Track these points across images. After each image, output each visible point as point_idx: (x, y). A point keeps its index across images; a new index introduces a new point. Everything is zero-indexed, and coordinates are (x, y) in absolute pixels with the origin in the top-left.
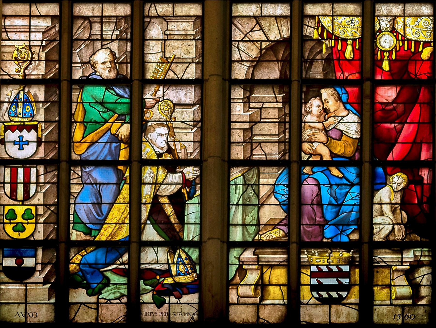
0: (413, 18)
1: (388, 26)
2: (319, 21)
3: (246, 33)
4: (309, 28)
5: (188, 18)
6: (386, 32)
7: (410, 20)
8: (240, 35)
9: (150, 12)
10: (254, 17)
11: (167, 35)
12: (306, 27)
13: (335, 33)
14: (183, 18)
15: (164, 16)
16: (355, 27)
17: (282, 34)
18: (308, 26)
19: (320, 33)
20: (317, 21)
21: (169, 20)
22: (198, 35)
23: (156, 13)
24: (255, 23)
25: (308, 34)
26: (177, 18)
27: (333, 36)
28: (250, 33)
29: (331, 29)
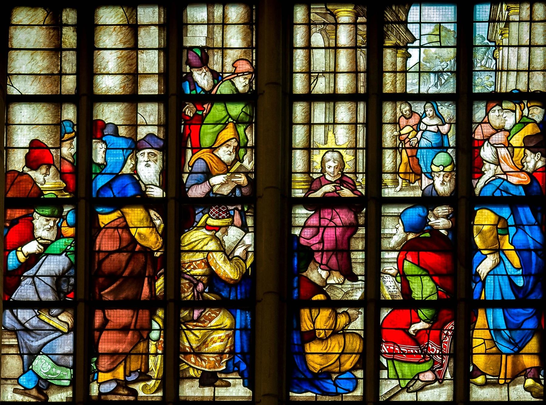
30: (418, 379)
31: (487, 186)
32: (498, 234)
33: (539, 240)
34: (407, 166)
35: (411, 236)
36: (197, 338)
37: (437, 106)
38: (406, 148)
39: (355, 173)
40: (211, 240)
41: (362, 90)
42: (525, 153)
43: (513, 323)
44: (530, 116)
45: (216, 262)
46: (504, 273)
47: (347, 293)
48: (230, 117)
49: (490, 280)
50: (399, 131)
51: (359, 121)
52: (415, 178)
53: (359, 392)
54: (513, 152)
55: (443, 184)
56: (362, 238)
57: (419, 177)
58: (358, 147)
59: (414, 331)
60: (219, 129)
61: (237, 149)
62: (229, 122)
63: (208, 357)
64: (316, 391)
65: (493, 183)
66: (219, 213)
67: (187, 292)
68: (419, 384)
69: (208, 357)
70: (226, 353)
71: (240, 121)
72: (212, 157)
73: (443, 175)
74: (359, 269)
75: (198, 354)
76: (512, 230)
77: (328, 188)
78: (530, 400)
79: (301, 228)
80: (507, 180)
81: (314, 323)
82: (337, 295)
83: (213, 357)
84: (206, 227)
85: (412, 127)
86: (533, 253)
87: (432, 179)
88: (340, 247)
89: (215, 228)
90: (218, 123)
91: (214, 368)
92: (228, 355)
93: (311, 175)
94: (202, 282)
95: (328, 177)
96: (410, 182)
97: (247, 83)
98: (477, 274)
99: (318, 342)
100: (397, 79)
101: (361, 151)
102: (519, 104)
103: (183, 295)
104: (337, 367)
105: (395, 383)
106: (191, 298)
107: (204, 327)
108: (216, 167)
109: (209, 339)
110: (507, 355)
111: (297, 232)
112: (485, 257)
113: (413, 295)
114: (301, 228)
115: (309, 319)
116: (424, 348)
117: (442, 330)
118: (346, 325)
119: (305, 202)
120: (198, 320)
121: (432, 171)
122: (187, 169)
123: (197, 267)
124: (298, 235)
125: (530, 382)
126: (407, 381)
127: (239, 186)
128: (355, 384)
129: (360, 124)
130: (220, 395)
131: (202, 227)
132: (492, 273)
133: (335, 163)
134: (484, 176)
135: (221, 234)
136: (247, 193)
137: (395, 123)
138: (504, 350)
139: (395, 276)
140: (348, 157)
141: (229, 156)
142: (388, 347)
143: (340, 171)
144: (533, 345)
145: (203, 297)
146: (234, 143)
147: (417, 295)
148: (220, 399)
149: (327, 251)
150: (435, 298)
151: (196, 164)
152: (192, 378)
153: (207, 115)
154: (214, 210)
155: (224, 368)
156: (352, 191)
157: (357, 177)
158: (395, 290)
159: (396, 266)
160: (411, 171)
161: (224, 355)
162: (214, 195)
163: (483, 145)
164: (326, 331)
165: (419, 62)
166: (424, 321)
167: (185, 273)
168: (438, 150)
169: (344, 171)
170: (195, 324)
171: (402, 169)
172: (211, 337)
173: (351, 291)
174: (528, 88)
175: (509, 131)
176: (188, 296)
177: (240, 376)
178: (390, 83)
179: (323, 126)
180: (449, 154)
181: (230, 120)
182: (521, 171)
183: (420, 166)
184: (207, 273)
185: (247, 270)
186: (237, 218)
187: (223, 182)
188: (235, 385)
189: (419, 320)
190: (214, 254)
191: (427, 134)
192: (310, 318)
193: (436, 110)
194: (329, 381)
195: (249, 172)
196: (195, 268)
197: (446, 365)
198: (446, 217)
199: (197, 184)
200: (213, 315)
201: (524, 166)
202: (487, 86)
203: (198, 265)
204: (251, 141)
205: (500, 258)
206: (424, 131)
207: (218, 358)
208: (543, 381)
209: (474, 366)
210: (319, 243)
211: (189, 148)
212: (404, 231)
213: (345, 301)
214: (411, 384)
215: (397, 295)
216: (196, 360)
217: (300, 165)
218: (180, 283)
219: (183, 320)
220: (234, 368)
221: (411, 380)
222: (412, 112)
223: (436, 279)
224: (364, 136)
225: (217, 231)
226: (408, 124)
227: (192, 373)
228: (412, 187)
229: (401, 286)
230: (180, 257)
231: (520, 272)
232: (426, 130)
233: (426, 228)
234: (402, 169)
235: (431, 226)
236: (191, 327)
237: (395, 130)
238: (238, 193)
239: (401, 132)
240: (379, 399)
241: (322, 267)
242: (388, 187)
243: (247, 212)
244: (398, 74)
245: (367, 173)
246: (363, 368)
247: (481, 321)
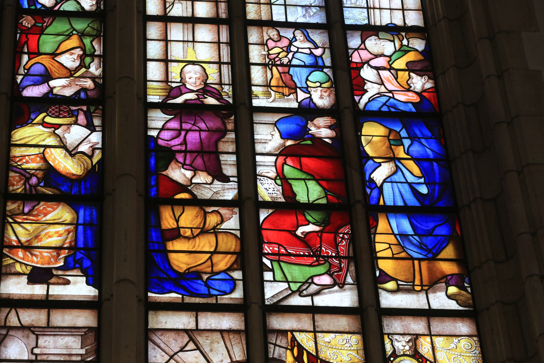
0: (445, 338)
1: (407, 348)
2: (294, 339)
3: (172, 353)
4: (277, 348)
5: (73, 330)
6: (405, 358)
7: (441, 340)
8: (162, 356)
9: (7, 320)
10: (186, 331)
11: (36, 355)
12: (272, 346)
13: (322, 356)
14: (65, 330)
15: (32, 327)
16: (353, 348)
17: (233, 356)
18: (275, 345)
19: (296, 355)
20: (289, 338)
21: (40, 333)
22: (89, 355)
23: (18, 322)
24: (186, 339)
25: (276, 356)
26: (55, 330)
27: (319, 361)
28: (180, 354)
29: (315, 350)
30: (313, 282)
31: (372, 102)
32: (391, 145)
33: (438, 151)
34: (279, 81)
35: (289, 143)
36: (27, 232)
37: (308, 33)
38: (277, 66)
39: (221, 84)
40: (50, 136)
41: (223, 15)
42: (409, 75)
43: (422, 230)
44: (410, 45)
45: (55, 158)
46: (403, 180)
47: (216, 193)
48: (74, 30)
49: (387, 187)
50: (268, 51)
51: (221, 41)
52: (289, 92)
53: (238, 294)
54: (397, 74)
55: (321, 97)
56: (232, 142)
57: (293, 91)
58: (222, 61)
59: (302, 233)
60: (61, 40)
61: (82, 58)
62: (73, 34)
63: (41, 253)
64: (183, 293)
65: (378, 99)
66: (59, 112)
67: (16, 185)
68: (313, 288)
69: (41, 253)
70: (65, 248)
71: (86, 34)
72: (53, 62)
73: (321, 91)
74: (230, 171)
75: (28, 248)
76: (407, 142)
77: (191, 96)
78: (456, 308)
79: (159, 130)
80: (393, 98)
81: (177, 221)
82: (205, 194)
83: (47, 252)
84: (44, 124)
85: (281, 48)
86: (435, 164)
87: (309, 93)
88: (206, 149)
89: (55, 126)
90: (61, 34)
91: (49, 264)
92: (67, 251)
93: (169, 84)
94: (36, 176)
95: (188, 86)
97: (94, 3)
98: (372, 181)
99: (183, 240)
100: (261, 9)
101: (226, 66)
102: (397, 35)
103: (11, 188)
104: (209, 267)
105: (285, 285)
106: (22, 191)
107: (37, 220)
108: (57, 71)
109: (43, 233)
110: (420, 260)
111: (154, 133)
112: (377, 165)
113: (298, 198)
114: (159, 130)
115: (171, 217)
116: (317, 251)
117: (336, 234)
118: (218, 225)
119: (163, 106)
120: (29, 214)
121: (308, 87)
122: (22, 71)
123: (31, 162)
124: (155, 137)
125: (453, 290)
126: (299, 285)
127: (84, 89)
128: (232, 286)
129: (223, 43)
130: (55, 293)
131: (38, 124)
132: (389, 180)
133: (196, 74)
134: (367, 93)
135: (61, 132)
136: (94, 96)
137: (263, 44)
138: (415, 255)
139: (275, 179)
140: (212, 70)
141: (73, 63)
142: (271, 248)
143: (203, 81)
144: (449, 252)
145: (36, 190)
146: (79, 52)
147: (302, 197)
148: (56, 298)
149: (191, 152)
150: (324, 201)
151: (33, 68)
152: (18, 274)
153: (47, 27)
154: (53, 110)
155: (62, 264)
156: (218, 99)
157: (222, 88)
158: (275, 192)
159: (274, 169)
160: (284, 85)
161: (63, 251)
162: (54, 96)
163: (362, 67)
164: (193, 229)
166: (313, 224)
167: (16, 167)
168: (313, 69)
169: (207, 82)
170: (25, 217)
171: (273, 83)
172: (46, 231)
173: (222, 191)
174: (405, 23)
175: (390, 57)
176: (18, 189)
177: (82, 273)
179: (182, 43)
180: (326, 73)
181: (74, 32)
182: (408, 90)
183: (294, 81)
184: (44, 167)
185: (93, 167)
186: (82, 118)
187: (65, 85)
188: (75, 283)
189: (308, 223)
190: (52, 149)
191: (298, 55)
192: (173, 217)
193: (307, 36)
194: (199, 282)
195: (97, 77)
196: (27, 162)
197: (345, 270)
198: (330, 127)
199: (35, 85)
200: (49, 209)
201: (411, 87)
202: (360, 20)
203: (32, 159)
204: (99, 51)
205: (397, 166)
206: (295, 53)
207: (55, 254)
208: (469, 289)
209: (381, 271)
210: (181, 144)
211: (25, 53)
212: (282, 137)
213: (215, 200)
214: (304, 287)
215: (278, 197)
216: (24, 255)
217: (156, 75)
218: (7, 176)
219: (10, 212)
220: (75, 265)
221: (304, 283)
222: (280, 37)
223: (324, 183)
224: (228, 53)
225: (56, 129)
227: (18, 268)
228: (287, 99)
229: (282, 189)
230: (9, 151)
231: (422, 180)
232: (297, 52)
233: (306, 136)
234: (273, 83)
235: (313, 135)
236: (20, 221)
238: (82, 95)
240: (265, 302)
241: (185, 167)
242: (259, 98)
243: (94, 112)
244: (262, 5)
245: (234, 84)
246: (243, 268)
247: (382, 225)
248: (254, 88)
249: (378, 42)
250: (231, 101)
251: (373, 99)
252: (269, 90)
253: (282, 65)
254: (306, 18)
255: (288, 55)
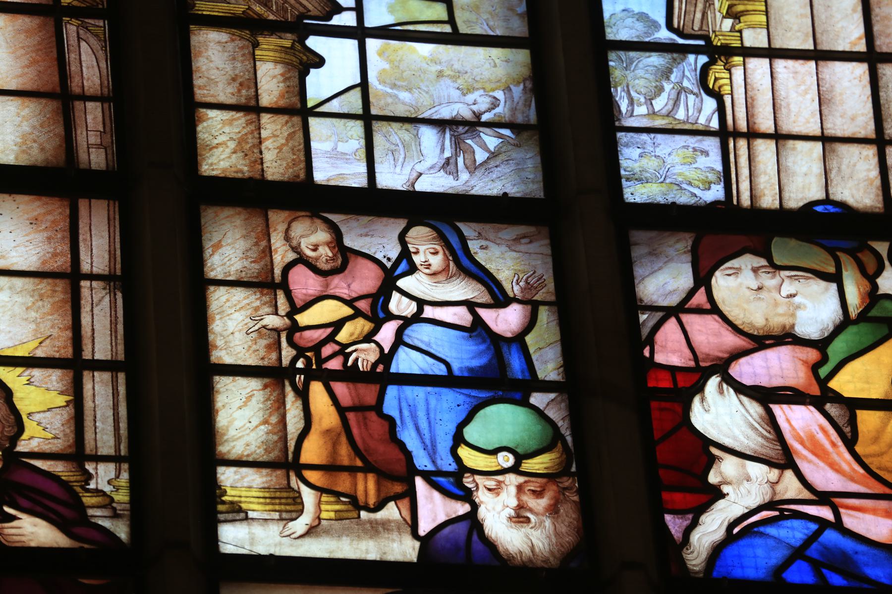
31: (743, 542)
34: (335, 445)
37: (463, 240)
38: (327, 378)
50: (290, 315)
51: (85, 267)
52: (378, 490)
54: (853, 422)
55: (520, 517)
57: (398, 488)
58: (87, 355)
65: (771, 530)
73: (520, 488)
80: (838, 525)
85: (349, 303)
87: (467, 496)
96: (356, 505)
100: (264, 134)
102: (852, 253)
121: (463, 469)
129: (91, 277)
134: (721, 504)
157: (87, 472)
160: (359, 463)
163: (699, 388)
165: (364, 85)
168: (484, 395)
175: (821, 345)
178: (232, 145)
183: (402, 446)
191: (420, 334)
193: (460, 253)
202: (690, 184)
206: (408, 322)
224: (113, 323)
226: (331, 292)
228: (370, 522)
232: (417, 318)
237: (267, 309)
239: (298, 317)
242: (247, 518)
244: (265, 118)
248: (227, 476)
249: (770, 281)
250: (122, 531)
251: (748, 531)
252: (294, 481)
253: (351, 374)
254: (455, 174)
255: (376, 330)
